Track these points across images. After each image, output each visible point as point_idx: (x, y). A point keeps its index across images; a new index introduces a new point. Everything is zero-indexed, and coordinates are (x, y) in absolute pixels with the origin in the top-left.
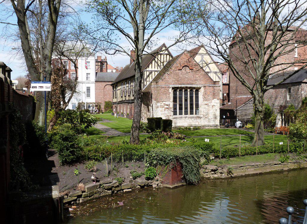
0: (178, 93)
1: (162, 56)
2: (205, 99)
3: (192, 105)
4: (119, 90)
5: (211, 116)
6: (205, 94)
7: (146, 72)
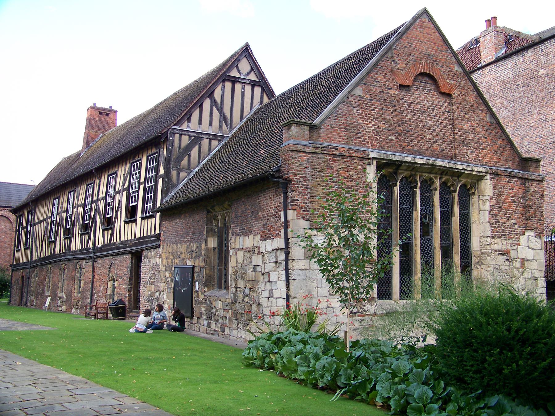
1: (238, 87)
2: (498, 230)
4: (41, 221)
7: (177, 136)
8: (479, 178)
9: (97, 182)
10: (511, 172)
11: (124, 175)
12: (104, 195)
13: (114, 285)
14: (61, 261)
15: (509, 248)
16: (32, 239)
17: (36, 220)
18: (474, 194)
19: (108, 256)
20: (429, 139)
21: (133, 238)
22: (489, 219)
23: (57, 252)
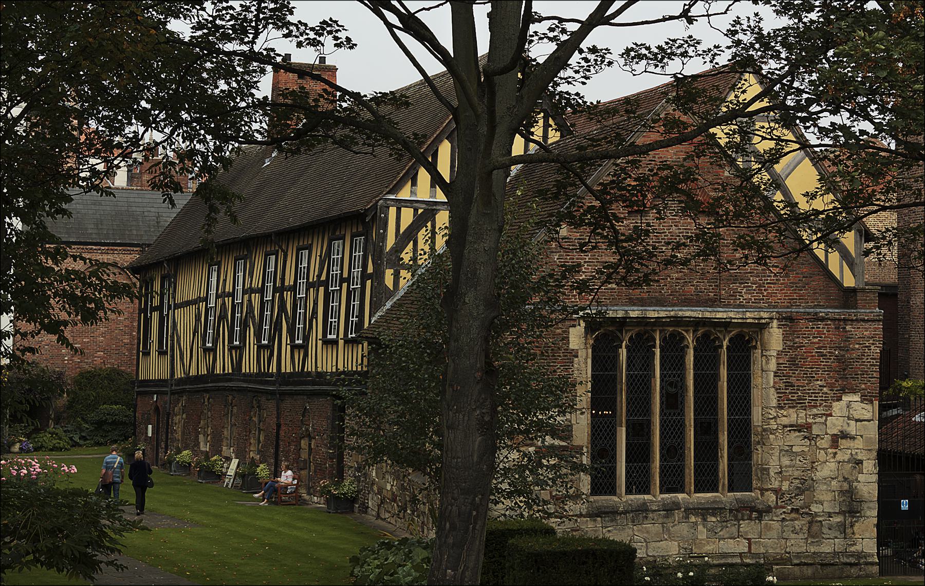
0: (623, 353)
2: (790, 397)
3: (707, 430)
4: (188, 303)
5: (825, 501)
6: (792, 360)
8: (761, 327)
9: (281, 255)
10: (816, 314)
11: (320, 256)
12: (292, 283)
13: (310, 444)
14: (225, 389)
15: (810, 421)
16: (172, 337)
17: (179, 300)
18: (755, 347)
19: (299, 394)
20: (677, 279)
21: (334, 370)
22: (775, 383)
23: (218, 371)
